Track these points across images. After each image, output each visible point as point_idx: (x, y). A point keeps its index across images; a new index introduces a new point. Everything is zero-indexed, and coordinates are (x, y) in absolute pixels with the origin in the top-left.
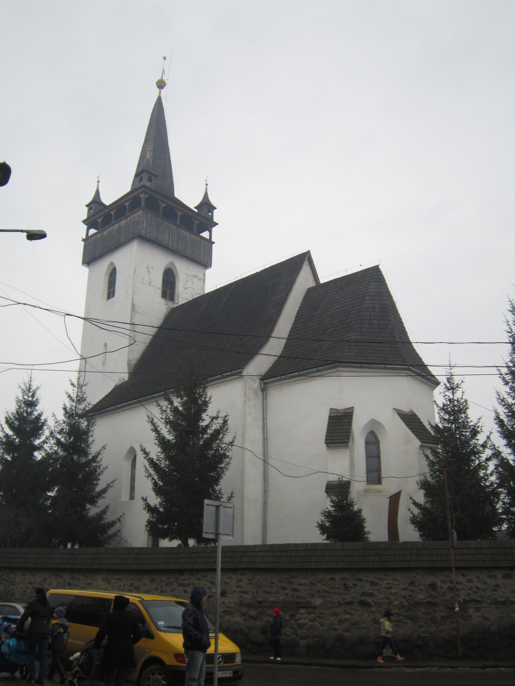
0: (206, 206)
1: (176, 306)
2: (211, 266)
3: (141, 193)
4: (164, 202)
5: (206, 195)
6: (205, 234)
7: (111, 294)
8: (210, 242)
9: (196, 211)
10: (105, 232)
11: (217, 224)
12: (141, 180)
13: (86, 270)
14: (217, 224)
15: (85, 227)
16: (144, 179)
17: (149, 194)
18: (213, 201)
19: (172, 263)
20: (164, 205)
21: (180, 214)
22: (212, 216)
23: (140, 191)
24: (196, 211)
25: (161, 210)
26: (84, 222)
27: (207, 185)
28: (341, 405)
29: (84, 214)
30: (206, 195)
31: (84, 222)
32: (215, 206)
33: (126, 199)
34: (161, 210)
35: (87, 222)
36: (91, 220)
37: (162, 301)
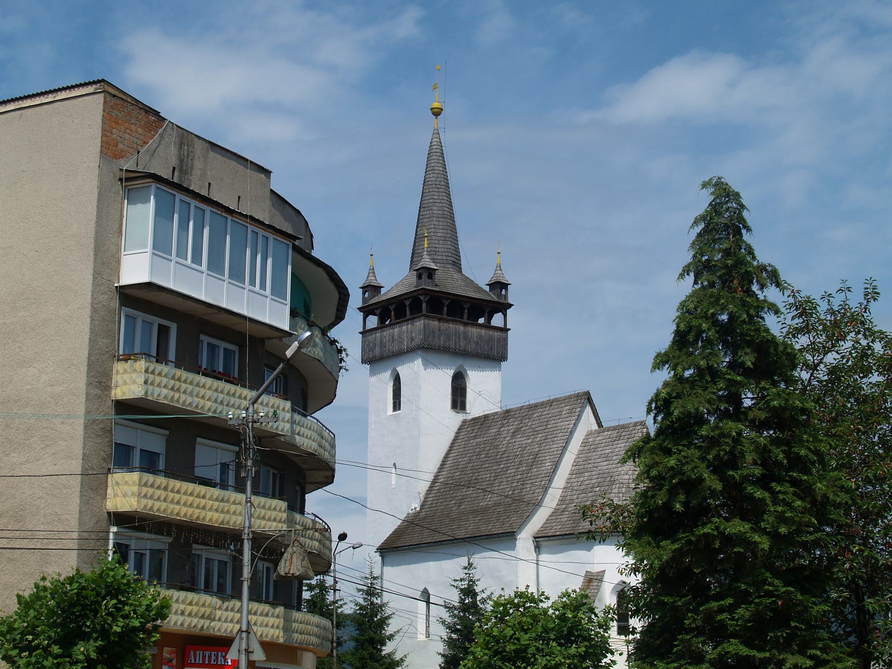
1: (469, 417)
3: (422, 295)
4: (447, 299)
6: (497, 320)
7: (397, 406)
8: (505, 330)
9: (487, 288)
10: (387, 333)
21: (466, 306)
22: (506, 297)
26: (360, 309)
28: (595, 569)
31: (360, 309)
33: (406, 297)
36: (367, 309)
37: (452, 414)
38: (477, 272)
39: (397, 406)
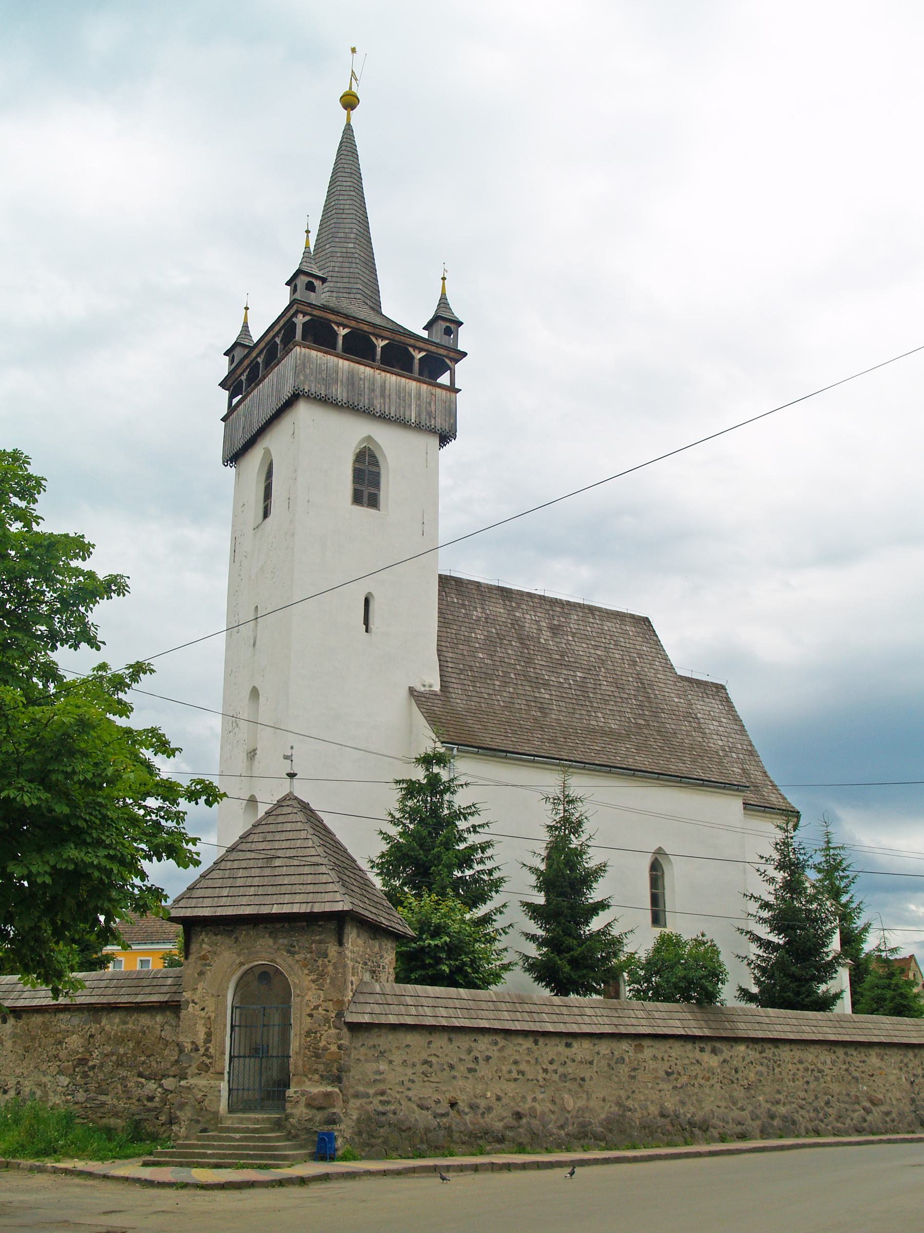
0: (445, 321)
2: (16, 457)
5: (443, 302)
8: (452, 389)
11: (464, 354)
12: (294, 291)
13: (231, 471)
14: (464, 354)
15: (226, 393)
16: (298, 287)
17: (310, 315)
18: (458, 312)
19: (369, 438)
20: (346, 331)
23: (292, 311)
24: (425, 334)
25: (340, 341)
27: (444, 279)
29: (222, 367)
30: (443, 302)
32: (461, 320)
34: (340, 341)
35: (229, 383)
38: (405, 306)
39: (266, 514)
